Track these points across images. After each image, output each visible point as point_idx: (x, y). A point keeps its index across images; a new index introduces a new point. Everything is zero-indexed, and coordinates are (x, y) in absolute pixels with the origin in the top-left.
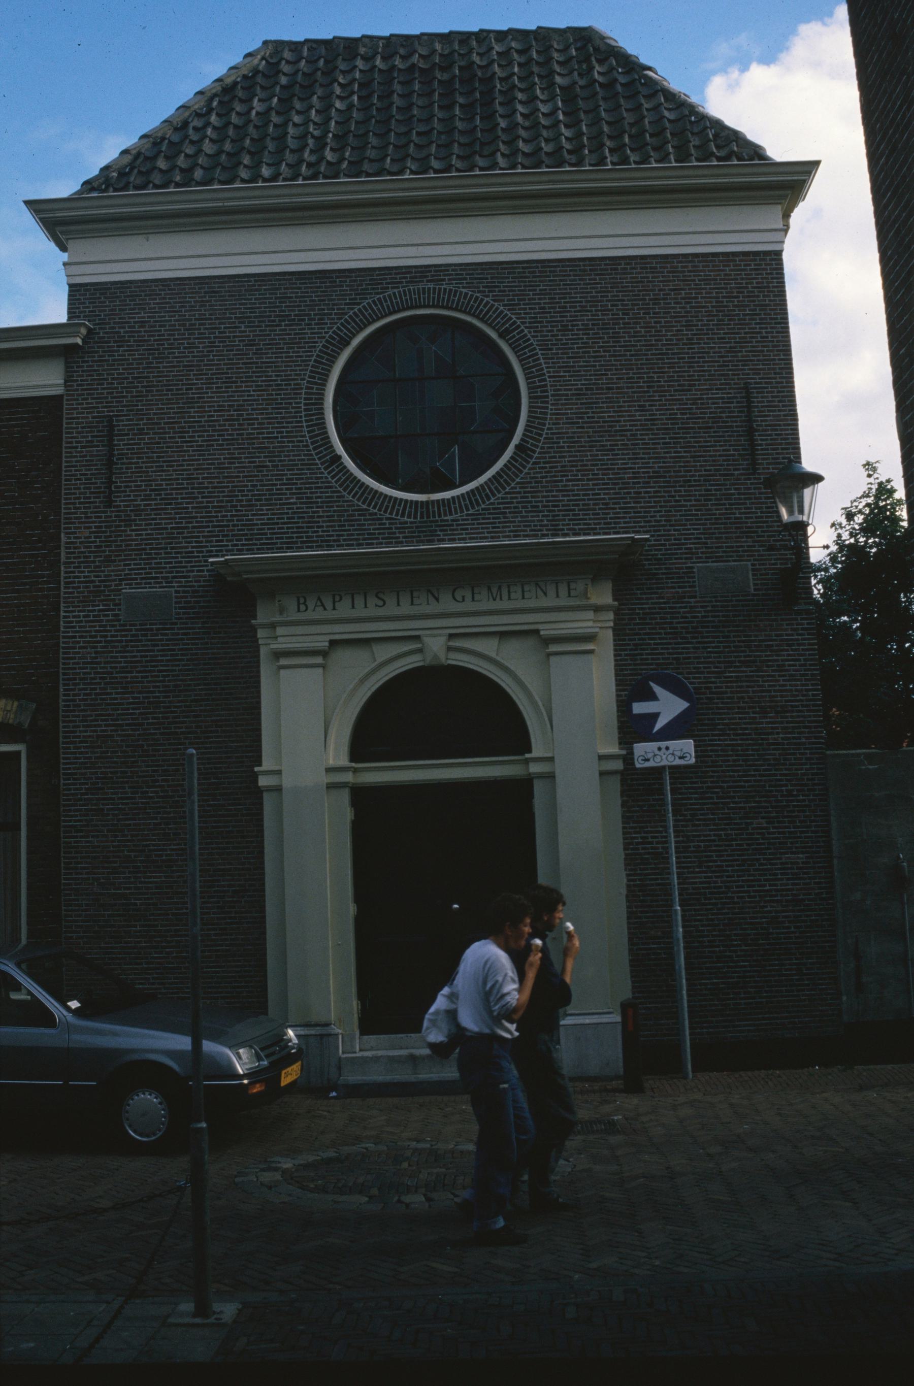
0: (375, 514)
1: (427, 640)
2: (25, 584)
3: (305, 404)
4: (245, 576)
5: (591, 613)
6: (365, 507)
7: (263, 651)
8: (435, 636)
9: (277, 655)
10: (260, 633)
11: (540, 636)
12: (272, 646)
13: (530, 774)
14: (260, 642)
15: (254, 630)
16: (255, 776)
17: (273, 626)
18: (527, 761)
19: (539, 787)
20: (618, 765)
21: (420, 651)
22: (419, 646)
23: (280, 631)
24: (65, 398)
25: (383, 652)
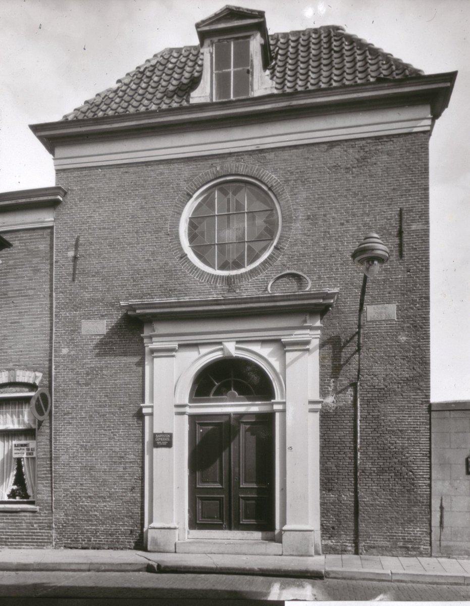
0: (203, 283)
1: (225, 344)
2: (37, 318)
3: (170, 228)
4: (138, 311)
5: (312, 333)
6: (197, 279)
7: (147, 349)
8: (228, 341)
9: (153, 351)
10: (145, 341)
11: (282, 342)
12: (150, 347)
13: (274, 410)
14: (145, 345)
15: (142, 339)
16: (141, 409)
17: (150, 337)
18: (272, 404)
19: (277, 415)
20: (319, 406)
21: (222, 349)
22: (222, 347)
23: (154, 339)
24: (55, 227)
25: (204, 350)
